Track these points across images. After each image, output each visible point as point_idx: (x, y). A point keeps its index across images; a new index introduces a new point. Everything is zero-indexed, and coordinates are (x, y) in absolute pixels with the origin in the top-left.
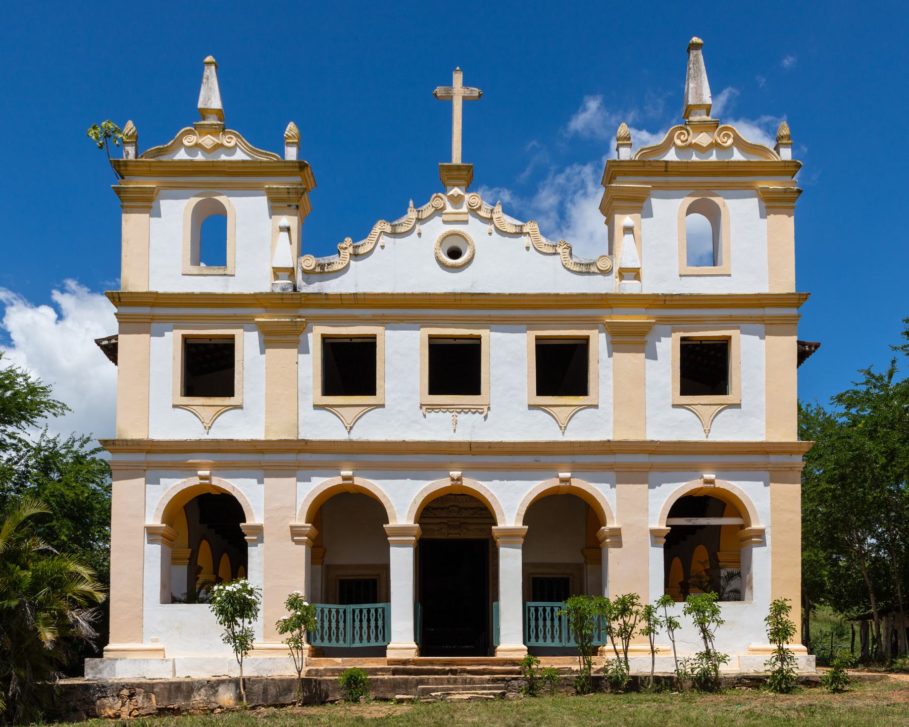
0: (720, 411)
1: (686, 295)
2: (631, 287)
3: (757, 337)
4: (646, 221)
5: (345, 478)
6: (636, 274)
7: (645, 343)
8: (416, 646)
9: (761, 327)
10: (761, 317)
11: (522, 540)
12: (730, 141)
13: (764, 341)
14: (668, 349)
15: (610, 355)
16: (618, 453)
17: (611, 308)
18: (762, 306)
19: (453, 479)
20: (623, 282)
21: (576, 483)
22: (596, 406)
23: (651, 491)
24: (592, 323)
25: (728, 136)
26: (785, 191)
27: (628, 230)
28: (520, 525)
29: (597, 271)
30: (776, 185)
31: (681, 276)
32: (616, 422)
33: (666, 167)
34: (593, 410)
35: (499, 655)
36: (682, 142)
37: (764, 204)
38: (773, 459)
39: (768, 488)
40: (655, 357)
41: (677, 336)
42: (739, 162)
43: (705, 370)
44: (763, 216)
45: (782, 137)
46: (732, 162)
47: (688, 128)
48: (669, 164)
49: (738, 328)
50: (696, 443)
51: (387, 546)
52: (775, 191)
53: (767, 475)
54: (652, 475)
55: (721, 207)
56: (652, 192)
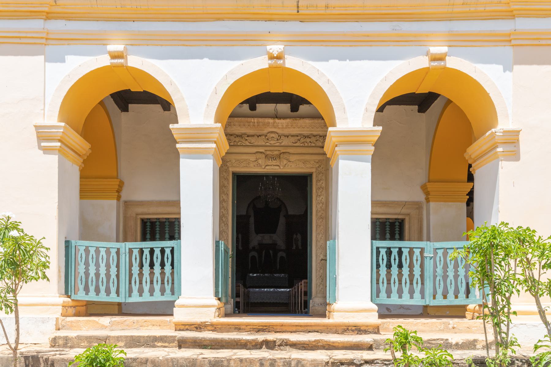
5: (114, 56)
8: (216, 302)
11: (373, 148)
16: (520, 16)
19: (271, 57)
21: (453, 63)
28: (369, 125)
35: (336, 318)
51: (176, 155)
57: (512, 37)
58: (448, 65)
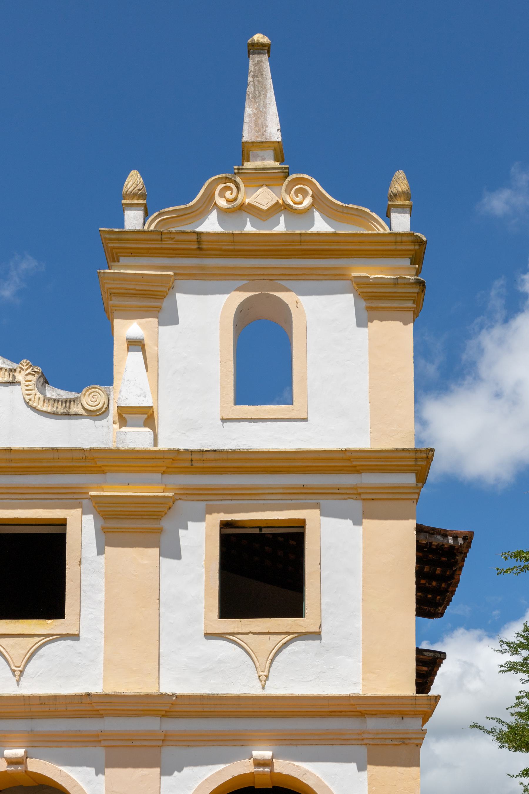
0: (285, 645)
1: (227, 452)
2: (137, 438)
3: (349, 522)
4: (166, 331)
6: (147, 417)
7: (160, 531)
9: (356, 505)
10: (355, 488)
12: (308, 201)
13: (360, 529)
14: (200, 541)
15: (101, 552)
16: (108, 715)
17: (104, 472)
18: (356, 470)
20: (124, 429)
22: (75, 637)
23: (165, 779)
24: (73, 497)
25: (304, 193)
26: (396, 282)
27: (136, 344)
29: (82, 412)
30: (382, 272)
31: (223, 420)
32: (107, 662)
33: (199, 242)
34: (69, 642)
36: (228, 201)
37: (363, 304)
38: (372, 724)
39: (365, 775)
40: (176, 555)
41: (214, 520)
42: (319, 234)
43: (263, 575)
44: (361, 323)
45: (395, 195)
46: (312, 234)
47: (238, 179)
48: (204, 238)
49: (316, 506)
50: (238, 698)
52: (378, 283)
53: (363, 751)
54: (169, 753)
55: (292, 307)
56: (178, 282)
57: (101, 738)
58: (30, 769)
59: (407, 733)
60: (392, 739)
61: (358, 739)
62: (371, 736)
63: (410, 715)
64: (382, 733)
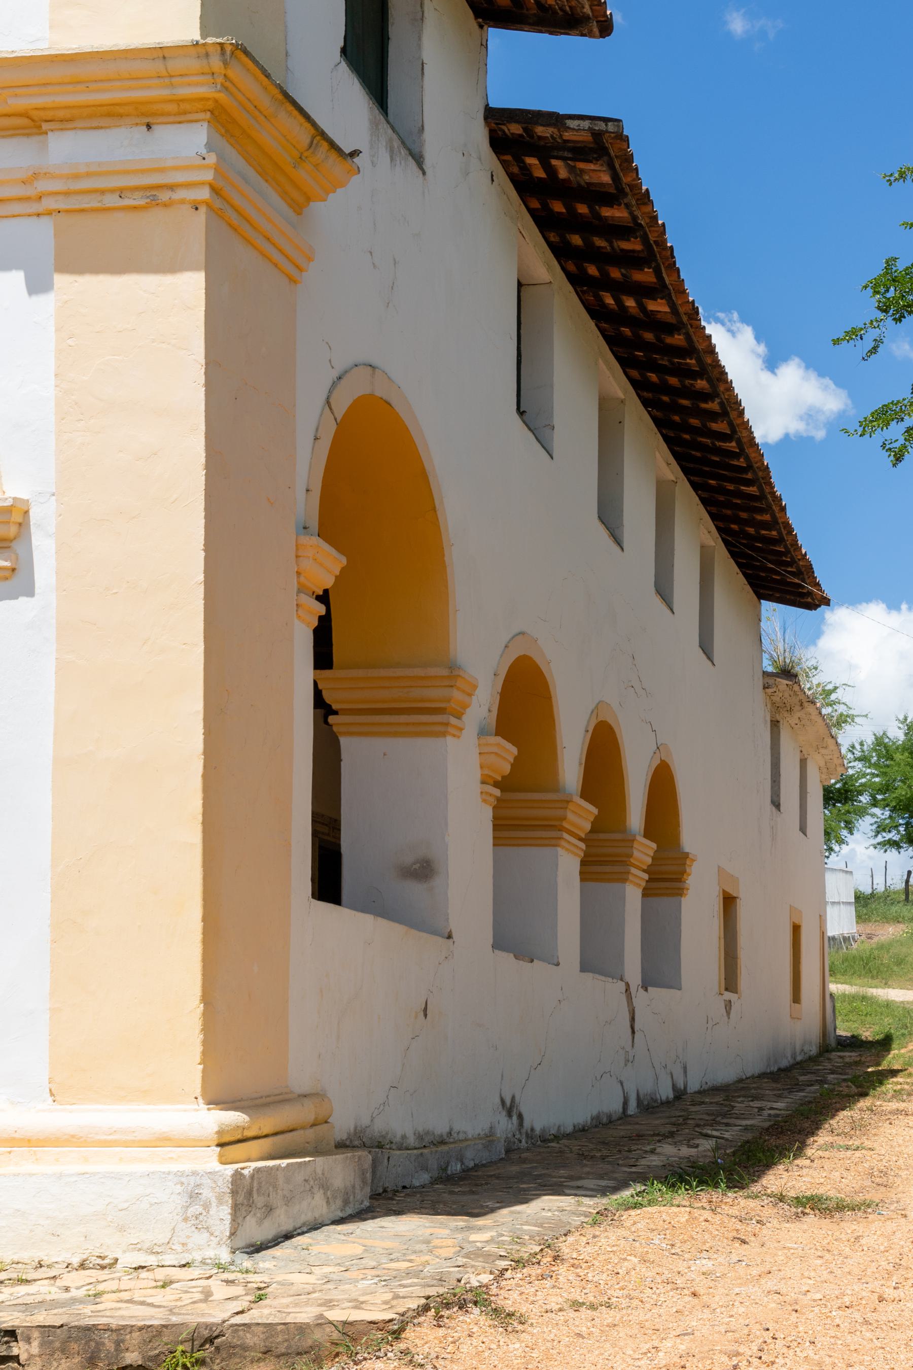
39: (47, 303)
53: (40, 234)
59: (162, 170)
60: (121, 192)
61: (28, 199)
62: (58, 186)
63: (169, 114)
64: (89, 175)
